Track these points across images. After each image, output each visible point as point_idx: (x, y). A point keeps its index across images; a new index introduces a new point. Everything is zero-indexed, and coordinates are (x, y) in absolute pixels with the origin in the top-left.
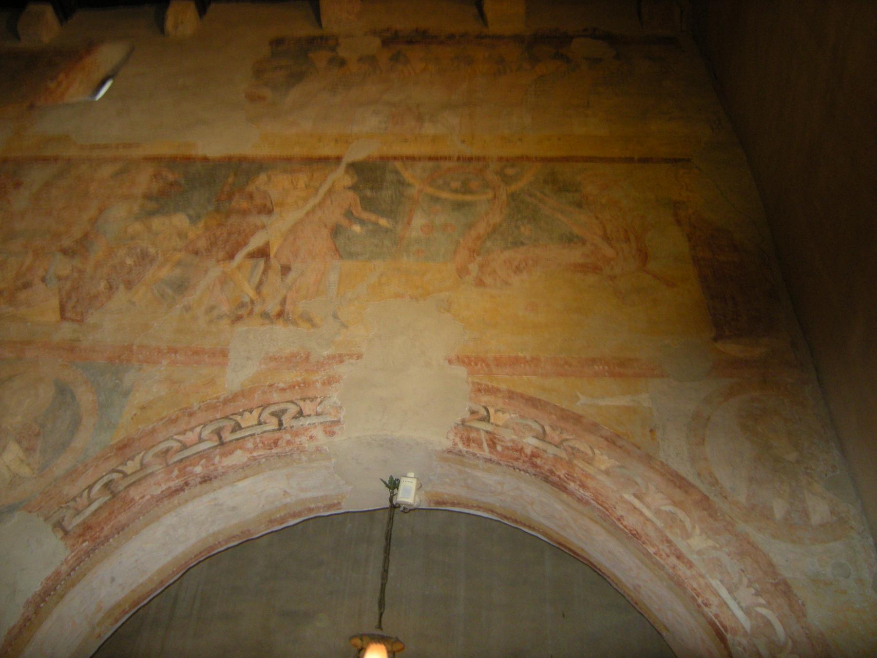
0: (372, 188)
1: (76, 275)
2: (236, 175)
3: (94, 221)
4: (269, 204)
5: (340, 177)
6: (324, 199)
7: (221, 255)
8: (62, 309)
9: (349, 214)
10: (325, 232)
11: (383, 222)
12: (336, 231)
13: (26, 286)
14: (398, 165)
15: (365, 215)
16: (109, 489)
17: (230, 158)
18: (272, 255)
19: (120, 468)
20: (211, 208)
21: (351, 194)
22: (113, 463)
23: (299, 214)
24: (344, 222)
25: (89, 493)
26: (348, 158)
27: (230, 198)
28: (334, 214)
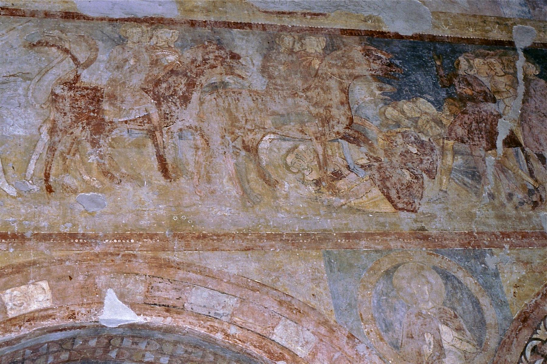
1: (376, 164)
3: (346, 102)
7: (484, 143)
8: (389, 198)
13: (338, 175)
16: (538, 354)
18: (523, 145)
19: (535, 336)
22: (526, 333)
25: (526, 358)
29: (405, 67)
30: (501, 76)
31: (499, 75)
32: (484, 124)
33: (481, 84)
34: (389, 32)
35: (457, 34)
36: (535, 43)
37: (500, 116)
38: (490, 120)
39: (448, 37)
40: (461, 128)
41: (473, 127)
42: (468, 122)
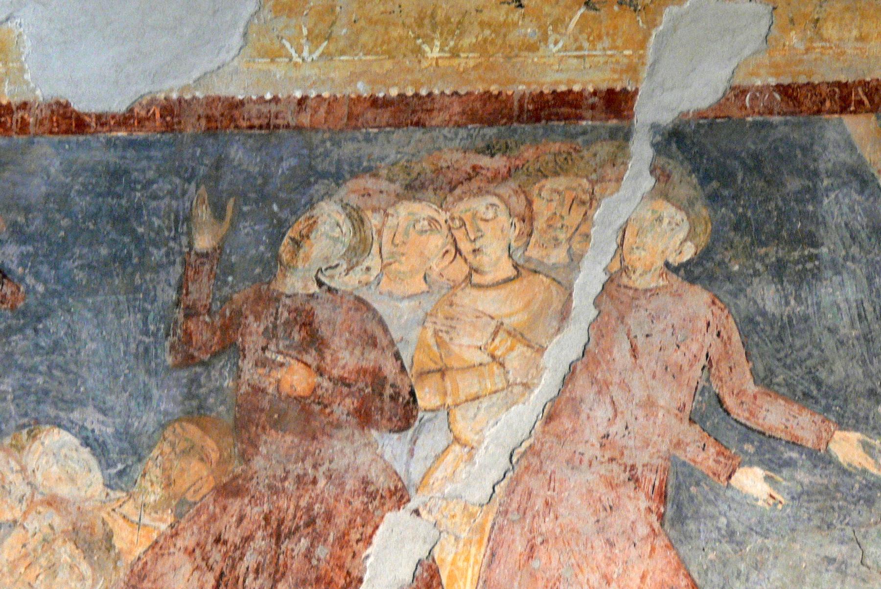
0: (779, 270)
2: (219, 212)
4: (390, 369)
5: (642, 219)
6: (599, 330)
9: (708, 410)
10: (636, 507)
11: (847, 447)
12: (676, 500)
14: (858, 126)
15: (775, 416)
17: (171, 113)
20: (167, 399)
21: (698, 299)
23: (524, 415)
24: (703, 456)
26: (654, 110)
27: (229, 345)
28: (647, 417)
29: (37, 275)
30: (496, 285)
31: (488, 279)
32: (304, 543)
33: (373, 333)
34: (24, 106)
35: (353, 78)
36: (740, 92)
37: (399, 496)
38: (341, 521)
39: (302, 102)
40: (188, 568)
41: (250, 560)
42: (233, 536)
